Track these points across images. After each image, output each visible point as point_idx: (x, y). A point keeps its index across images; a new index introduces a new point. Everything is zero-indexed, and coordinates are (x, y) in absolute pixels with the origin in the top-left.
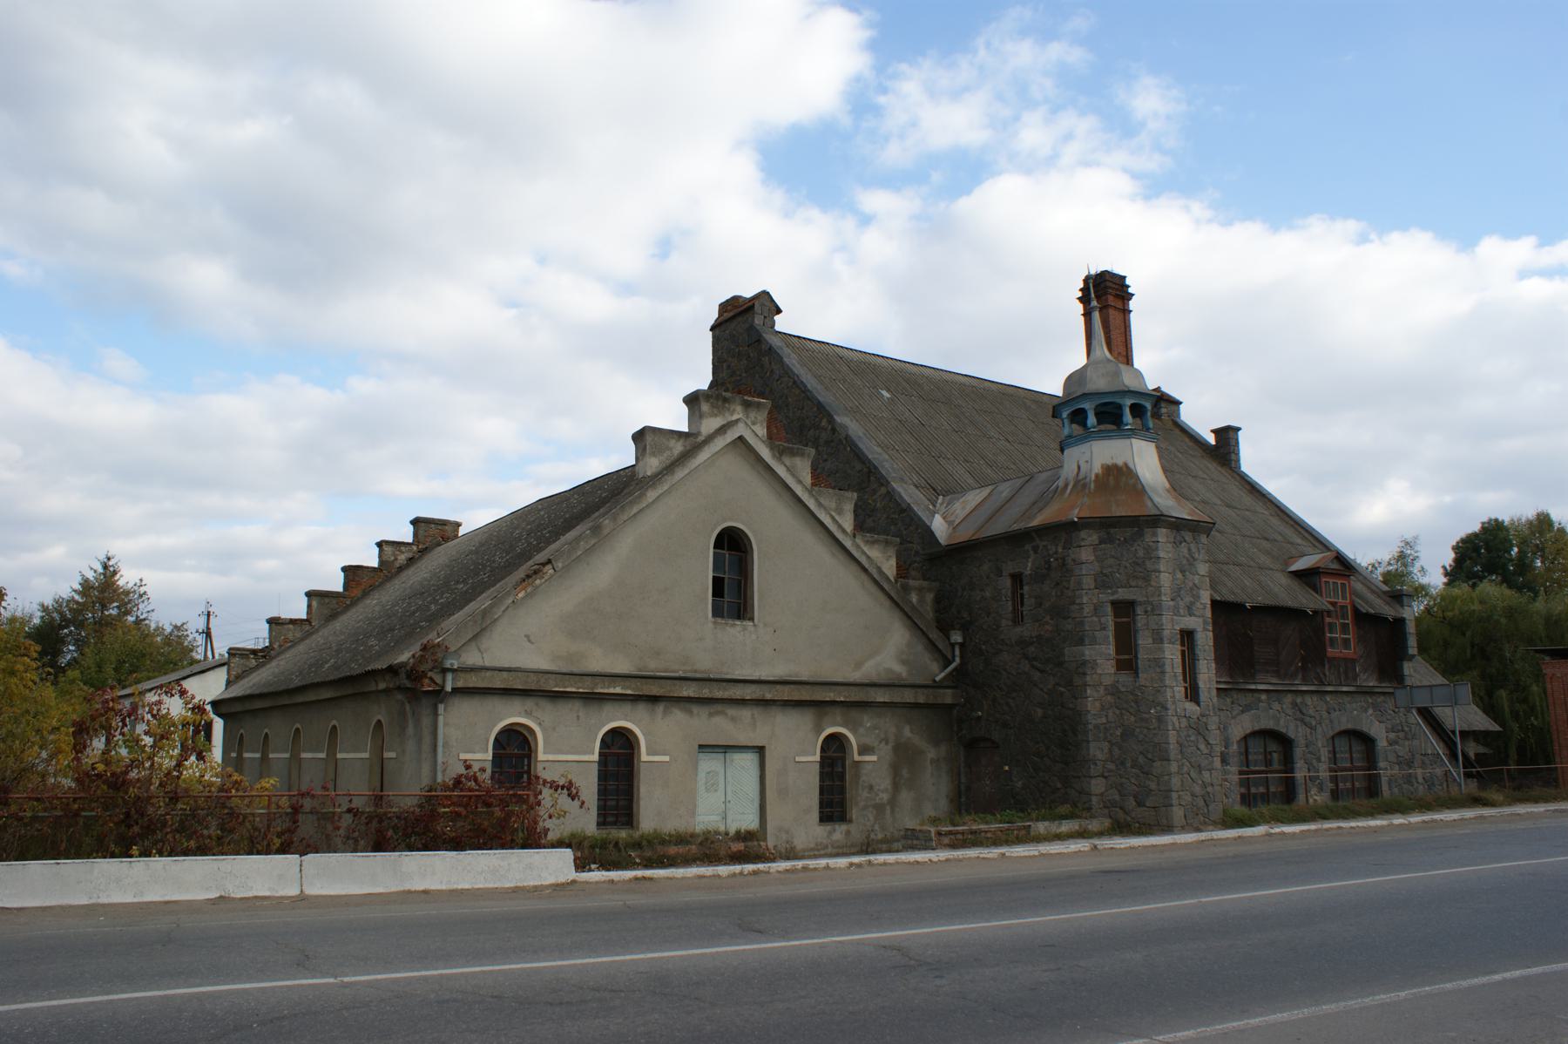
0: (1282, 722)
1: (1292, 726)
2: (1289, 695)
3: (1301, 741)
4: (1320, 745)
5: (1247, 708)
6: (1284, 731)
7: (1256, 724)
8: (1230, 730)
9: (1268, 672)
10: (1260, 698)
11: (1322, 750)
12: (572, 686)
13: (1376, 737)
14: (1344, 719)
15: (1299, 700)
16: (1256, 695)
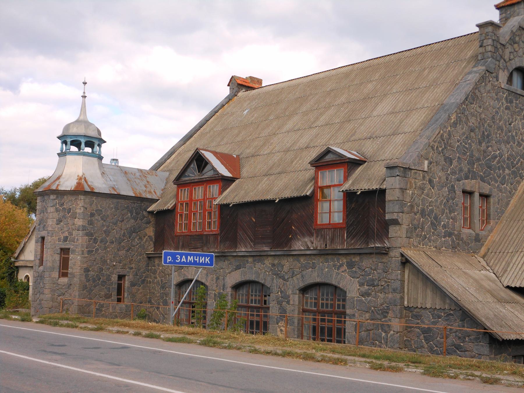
0: (261, 276)
1: (269, 279)
2: (270, 258)
3: (275, 289)
4: (290, 292)
5: (238, 268)
6: (262, 282)
7: (243, 277)
8: (226, 281)
9: (264, 243)
10: (248, 260)
11: (291, 296)
12: (30, 264)
13: (345, 289)
14: (316, 274)
15: (276, 262)
16: (246, 259)
